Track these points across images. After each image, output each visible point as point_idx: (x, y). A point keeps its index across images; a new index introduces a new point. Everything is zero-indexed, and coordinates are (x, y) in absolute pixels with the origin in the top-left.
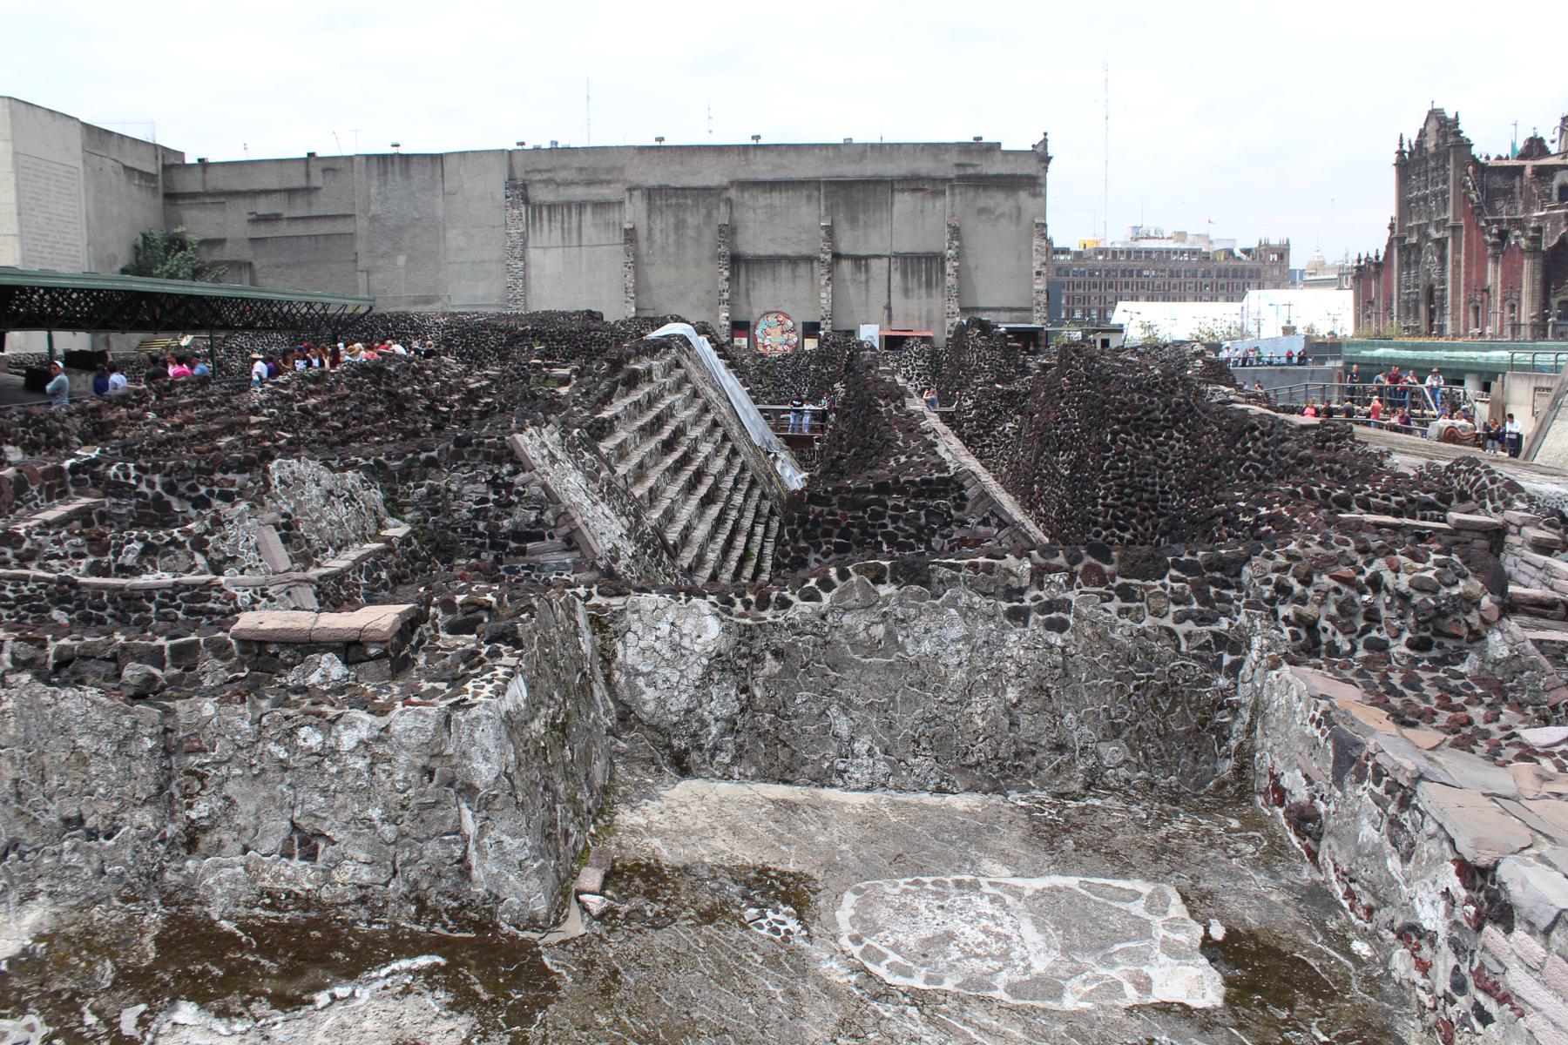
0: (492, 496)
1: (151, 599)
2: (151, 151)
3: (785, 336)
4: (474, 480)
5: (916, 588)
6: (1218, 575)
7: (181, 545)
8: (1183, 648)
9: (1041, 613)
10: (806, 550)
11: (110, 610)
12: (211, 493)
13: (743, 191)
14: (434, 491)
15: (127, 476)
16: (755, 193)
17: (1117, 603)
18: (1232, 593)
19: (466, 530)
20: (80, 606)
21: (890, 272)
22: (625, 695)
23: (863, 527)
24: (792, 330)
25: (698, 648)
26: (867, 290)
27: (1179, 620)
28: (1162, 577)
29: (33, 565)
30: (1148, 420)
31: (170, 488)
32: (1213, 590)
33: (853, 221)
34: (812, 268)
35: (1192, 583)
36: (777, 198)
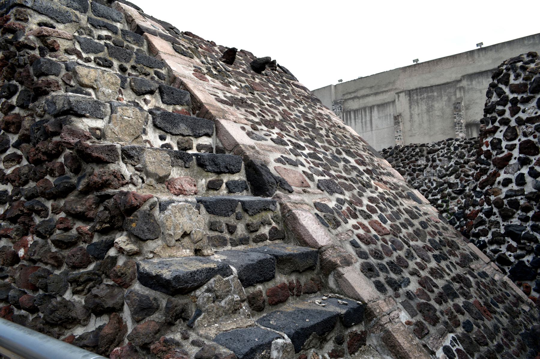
16: (480, 80)
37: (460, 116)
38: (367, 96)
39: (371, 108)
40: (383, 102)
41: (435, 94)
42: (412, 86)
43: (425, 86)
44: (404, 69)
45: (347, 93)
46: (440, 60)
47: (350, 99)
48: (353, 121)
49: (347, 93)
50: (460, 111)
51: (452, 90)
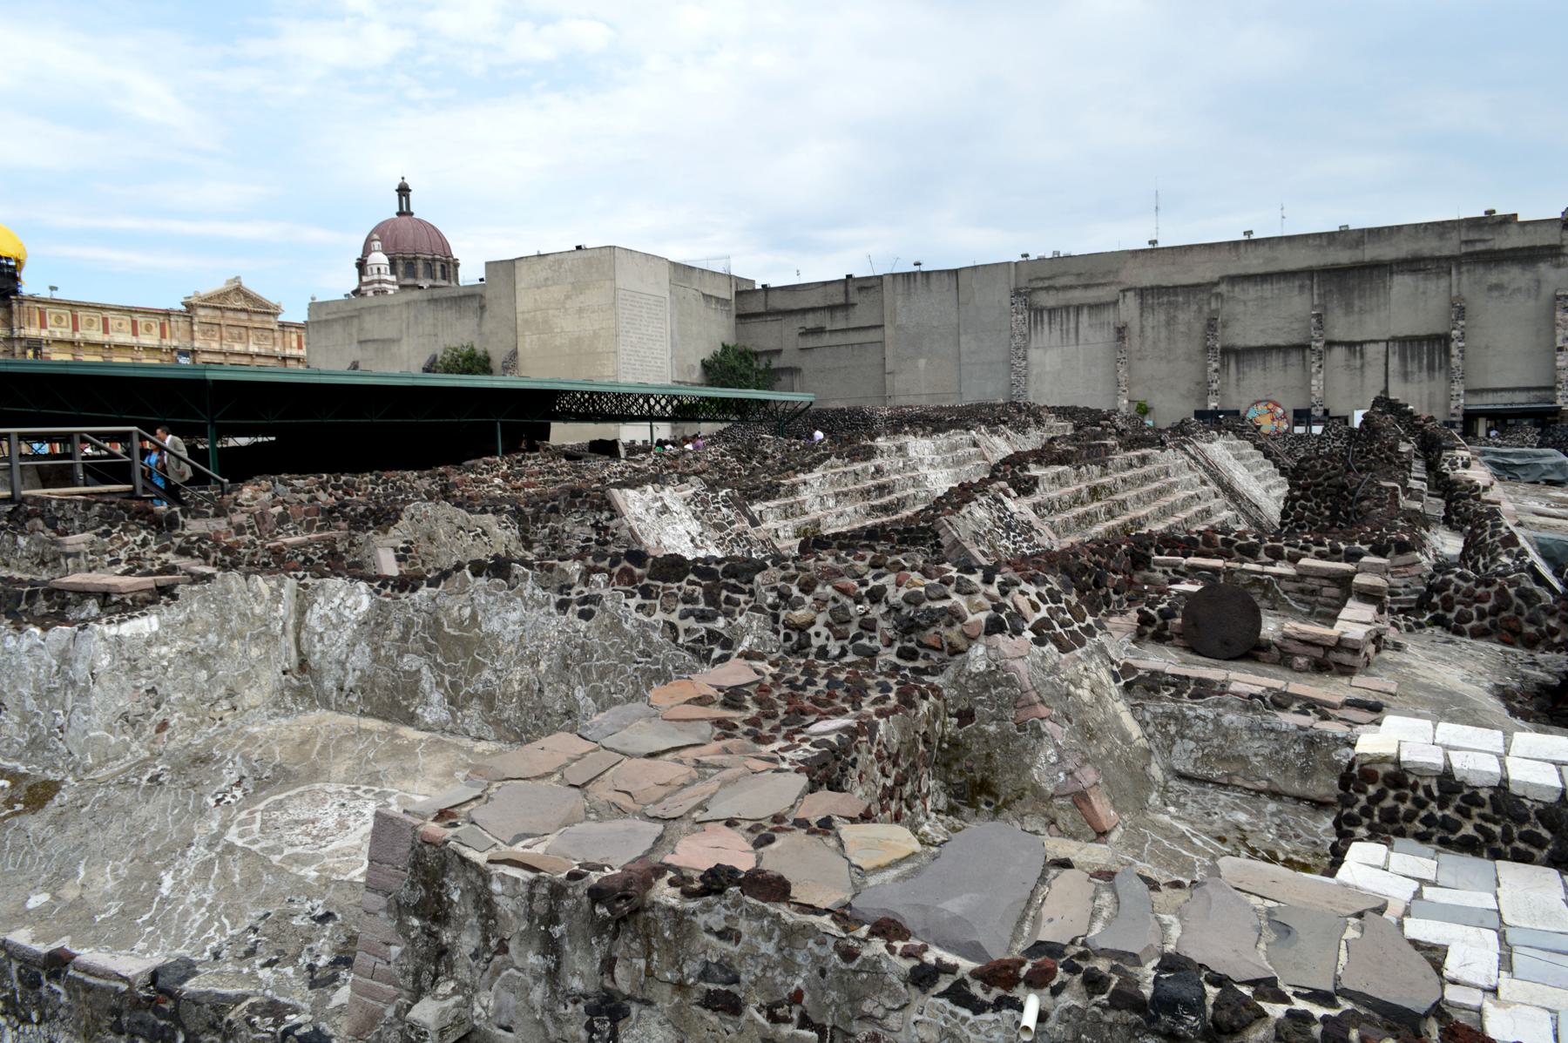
2: (727, 280)
3: (1276, 423)
5: (497, 580)
6: (732, 581)
8: (680, 641)
9: (579, 604)
13: (1233, 285)
14: (554, 531)
16: (1246, 287)
17: (638, 600)
18: (742, 598)
22: (305, 648)
24: (1284, 416)
25: (353, 617)
27: (683, 616)
28: (680, 580)
30: (1329, 485)
32: (724, 593)
33: (1348, 308)
34: (1304, 358)
35: (705, 588)
36: (1267, 290)
37: (1215, 338)
38: (1071, 287)
39: (1078, 308)
40: (1098, 301)
41: (1181, 299)
42: (1146, 283)
43: (1164, 283)
44: (1135, 253)
45: (1037, 279)
46: (1191, 247)
47: (1041, 289)
48: (1046, 327)
49: (1037, 279)
50: (1216, 330)
51: (1205, 296)
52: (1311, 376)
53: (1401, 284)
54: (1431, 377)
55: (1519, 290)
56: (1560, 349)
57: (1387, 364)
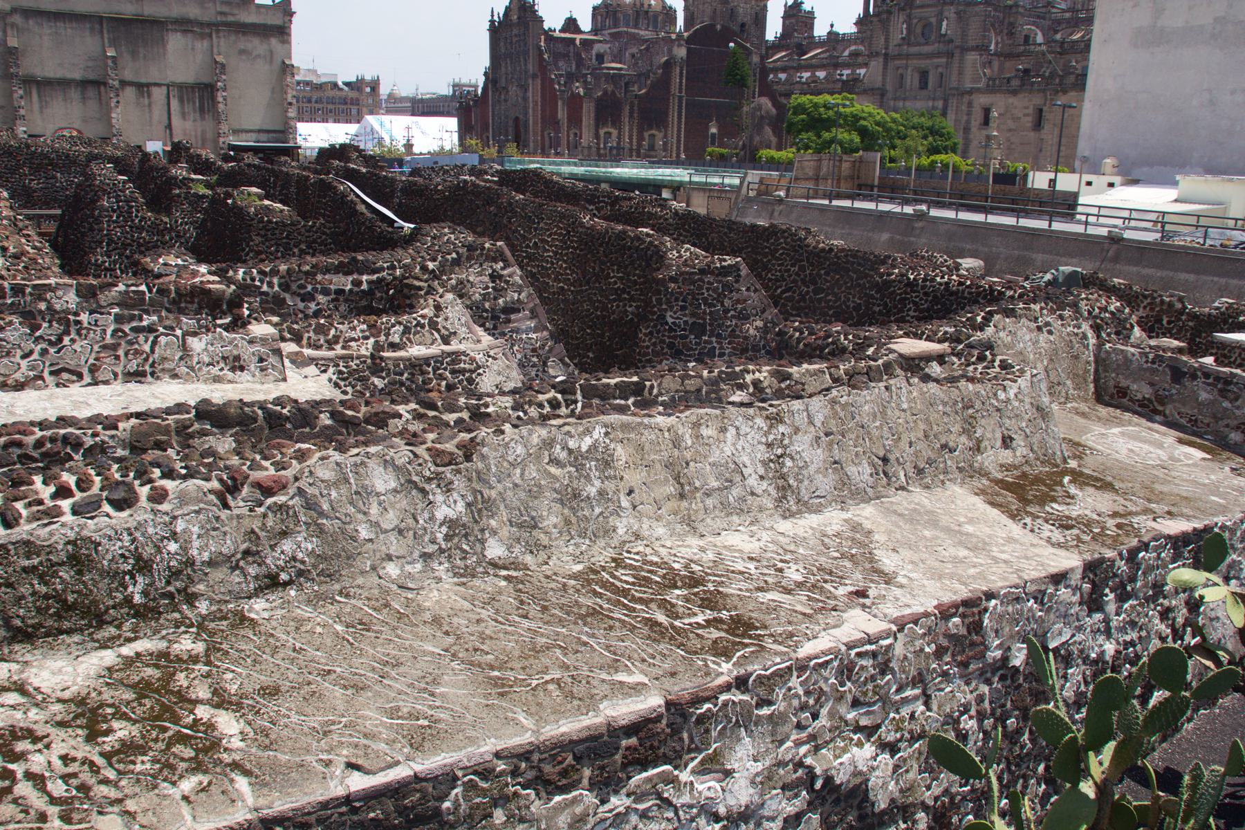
0: (491, 285)
1: (429, 365)
4: (480, 274)
7: (423, 326)
10: (666, 310)
11: (406, 375)
12: (315, 290)
15: (253, 279)
19: (478, 308)
20: (388, 375)
21: (168, 98)
23: (693, 294)
26: (150, 111)
29: (338, 347)
31: (285, 287)
33: (134, 54)
52: (109, 111)
53: (175, 42)
54: (203, 119)
55: (259, 56)
56: (290, 104)
57: (169, 104)
